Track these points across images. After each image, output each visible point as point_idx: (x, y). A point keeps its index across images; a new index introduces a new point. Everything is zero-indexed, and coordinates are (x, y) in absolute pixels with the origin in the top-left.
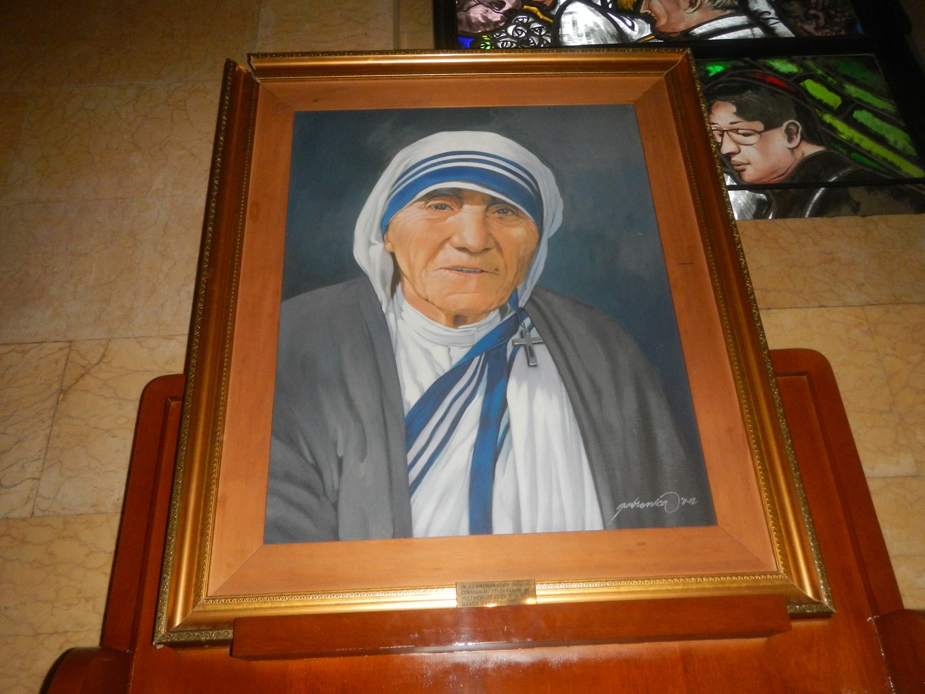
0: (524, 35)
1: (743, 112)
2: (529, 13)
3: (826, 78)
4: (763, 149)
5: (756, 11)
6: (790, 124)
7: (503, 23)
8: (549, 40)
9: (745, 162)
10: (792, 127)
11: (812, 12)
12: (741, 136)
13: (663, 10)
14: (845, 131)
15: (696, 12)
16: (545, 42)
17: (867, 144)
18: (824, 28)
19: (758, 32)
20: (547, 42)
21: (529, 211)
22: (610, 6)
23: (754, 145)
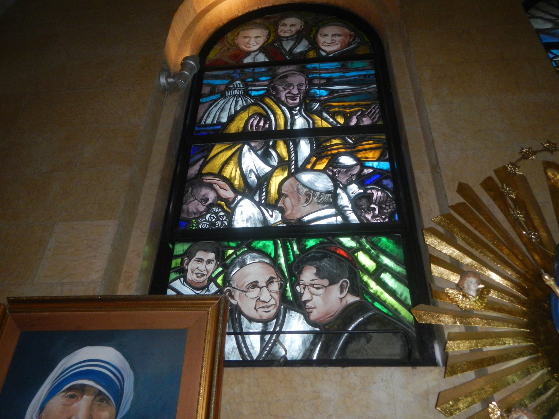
0: (214, 220)
1: (319, 274)
2: (220, 206)
3: (370, 251)
4: (325, 299)
5: (341, 205)
6: (343, 282)
7: (205, 212)
8: (226, 224)
10: (344, 284)
11: (373, 206)
12: (315, 289)
13: (291, 205)
14: (374, 287)
15: (308, 206)
16: (224, 225)
17: (385, 296)
18: (377, 216)
20: (225, 224)
21: (114, 400)
22: (263, 202)
23: (322, 296)
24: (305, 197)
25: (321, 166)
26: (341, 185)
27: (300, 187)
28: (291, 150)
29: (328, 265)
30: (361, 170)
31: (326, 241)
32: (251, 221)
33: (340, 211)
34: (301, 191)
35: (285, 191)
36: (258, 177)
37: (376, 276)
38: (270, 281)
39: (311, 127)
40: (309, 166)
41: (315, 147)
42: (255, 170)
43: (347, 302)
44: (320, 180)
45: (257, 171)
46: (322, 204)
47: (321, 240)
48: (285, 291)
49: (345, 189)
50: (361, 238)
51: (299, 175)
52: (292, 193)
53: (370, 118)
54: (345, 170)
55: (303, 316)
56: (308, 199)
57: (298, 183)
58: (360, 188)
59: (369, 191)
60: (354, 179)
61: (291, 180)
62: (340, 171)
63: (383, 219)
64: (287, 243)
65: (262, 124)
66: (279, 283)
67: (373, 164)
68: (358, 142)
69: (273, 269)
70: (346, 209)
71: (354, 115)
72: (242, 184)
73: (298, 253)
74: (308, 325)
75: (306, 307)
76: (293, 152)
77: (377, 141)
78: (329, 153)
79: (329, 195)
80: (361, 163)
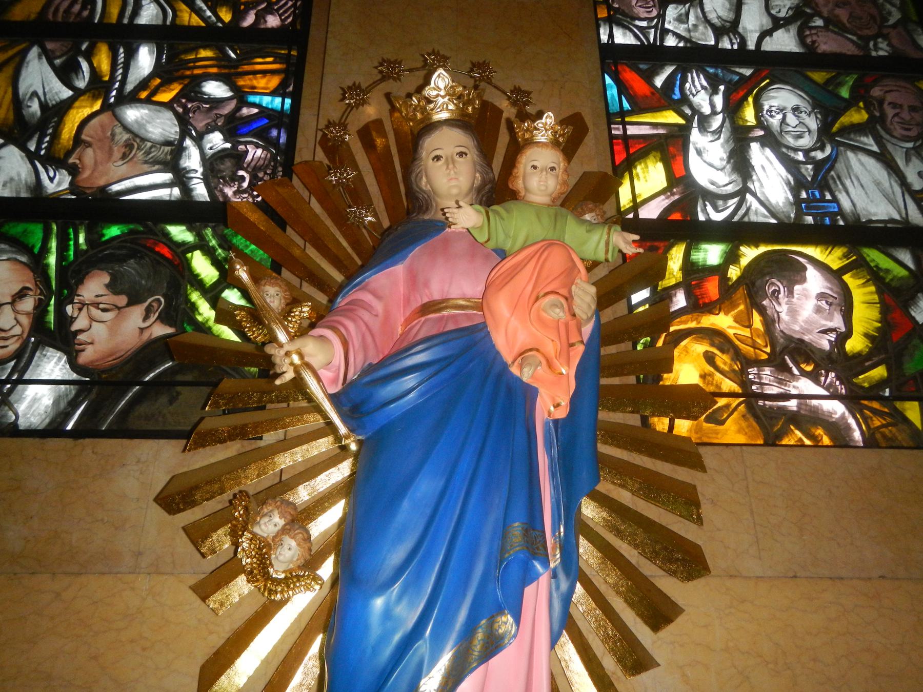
1: (113, 287)
4: (113, 329)
5: (185, 169)
9: (89, 341)
11: (241, 173)
12: (99, 311)
13: (93, 162)
15: (125, 165)
18: (245, 191)
19: (176, 192)
22: (43, 152)
23: (108, 323)
24: (123, 150)
25: (165, 97)
26: (193, 132)
27: (119, 130)
28: (120, 62)
29: (133, 271)
30: (238, 109)
31: (142, 229)
32: (11, 188)
33: (181, 178)
34: (117, 138)
35: (88, 136)
36: (44, 106)
37: (213, 294)
38: (21, 295)
39: (168, 23)
40: (143, 95)
41: (164, 60)
42: (40, 93)
43: (151, 334)
44: (158, 121)
45: (45, 94)
46: (151, 163)
47: (131, 226)
48: (45, 312)
49: (199, 141)
50: (206, 227)
51: (121, 109)
52: (100, 140)
53: (280, 16)
54: (208, 106)
55: (65, 358)
56: (128, 153)
57: (117, 123)
58: (226, 140)
59: (241, 147)
60: (219, 124)
61: (105, 117)
62: (199, 108)
63: (254, 197)
64: (68, 228)
65: (77, 8)
66: (37, 298)
67: (261, 100)
68: (246, 57)
69: (31, 274)
70: (192, 175)
71: (253, 8)
72: (11, 116)
73: (84, 247)
74: (72, 372)
75: (76, 342)
76: (119, 67)
77: (278, 59)
78: (188, 73)
79: (167, 149)
80: (240, 96)
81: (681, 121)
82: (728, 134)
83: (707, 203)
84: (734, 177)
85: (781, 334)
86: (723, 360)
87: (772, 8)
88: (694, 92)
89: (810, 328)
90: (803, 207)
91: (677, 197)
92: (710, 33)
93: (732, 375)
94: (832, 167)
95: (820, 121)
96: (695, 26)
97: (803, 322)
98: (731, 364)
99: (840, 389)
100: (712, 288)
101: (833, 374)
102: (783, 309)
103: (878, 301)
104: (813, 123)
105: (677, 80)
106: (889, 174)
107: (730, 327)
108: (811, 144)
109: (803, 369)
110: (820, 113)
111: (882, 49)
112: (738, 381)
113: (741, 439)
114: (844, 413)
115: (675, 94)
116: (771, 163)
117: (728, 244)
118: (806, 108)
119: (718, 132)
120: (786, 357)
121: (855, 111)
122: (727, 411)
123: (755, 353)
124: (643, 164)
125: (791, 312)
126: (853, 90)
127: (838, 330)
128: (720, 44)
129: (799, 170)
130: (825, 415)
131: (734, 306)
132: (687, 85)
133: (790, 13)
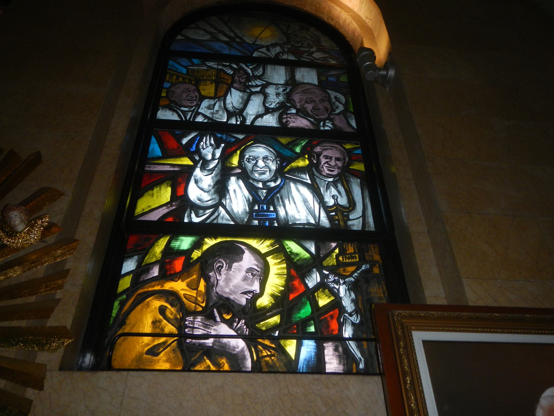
81: (191, 163)
82: (218, 171)
83: (192, 212)
84: (215, 196)
85: (216, 294)
86: (171, 311)
87: (267, 103)
88: (205, 147)
89: (236, 290)
90: (254, 215)
91: (174, 208)
92: (225, 115)
93: (174, 322)
94: (279, 192)
95: (278, 165)
96: (217, 111)
97: (233, 286)
98: (175, 315)
99: (245, 331)
100: (178, 264)
101: (244, 321)
102: (222, 278)
103: (286, 274)
104: (273, 167)
105: (196, 140)
106: (314, 196)
107: (183, 290)
108: (269, 178)
109: (223, 318)
110: (279, 161)
111: (327, 126)
112: (176, 325)
113: (167, 366)
114: (244, 347)
115: (192, 148)
116: (240, 188)
117: (197, 237)
118: (272, 158)
119: (213, 170)
120: (215, 310)
121: (301, 160)
122: (163, 346)
123: (195, 306)
124: (158, 188)
125: (226, 280)
126: (303, 149)
127: (254, 292)
128: (229, 121)
129: (257, 193)
130: (230, 349)
131: (189, 275)
132: (202, 143)
133: (277, 105)
